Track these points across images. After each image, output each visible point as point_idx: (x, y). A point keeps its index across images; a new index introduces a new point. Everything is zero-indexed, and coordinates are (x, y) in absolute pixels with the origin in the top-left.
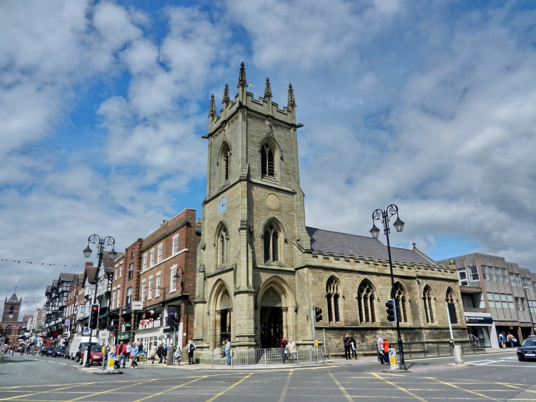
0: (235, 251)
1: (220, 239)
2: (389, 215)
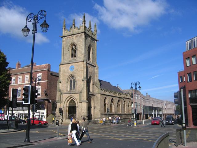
1: (69, 81)
2: (137, 84)
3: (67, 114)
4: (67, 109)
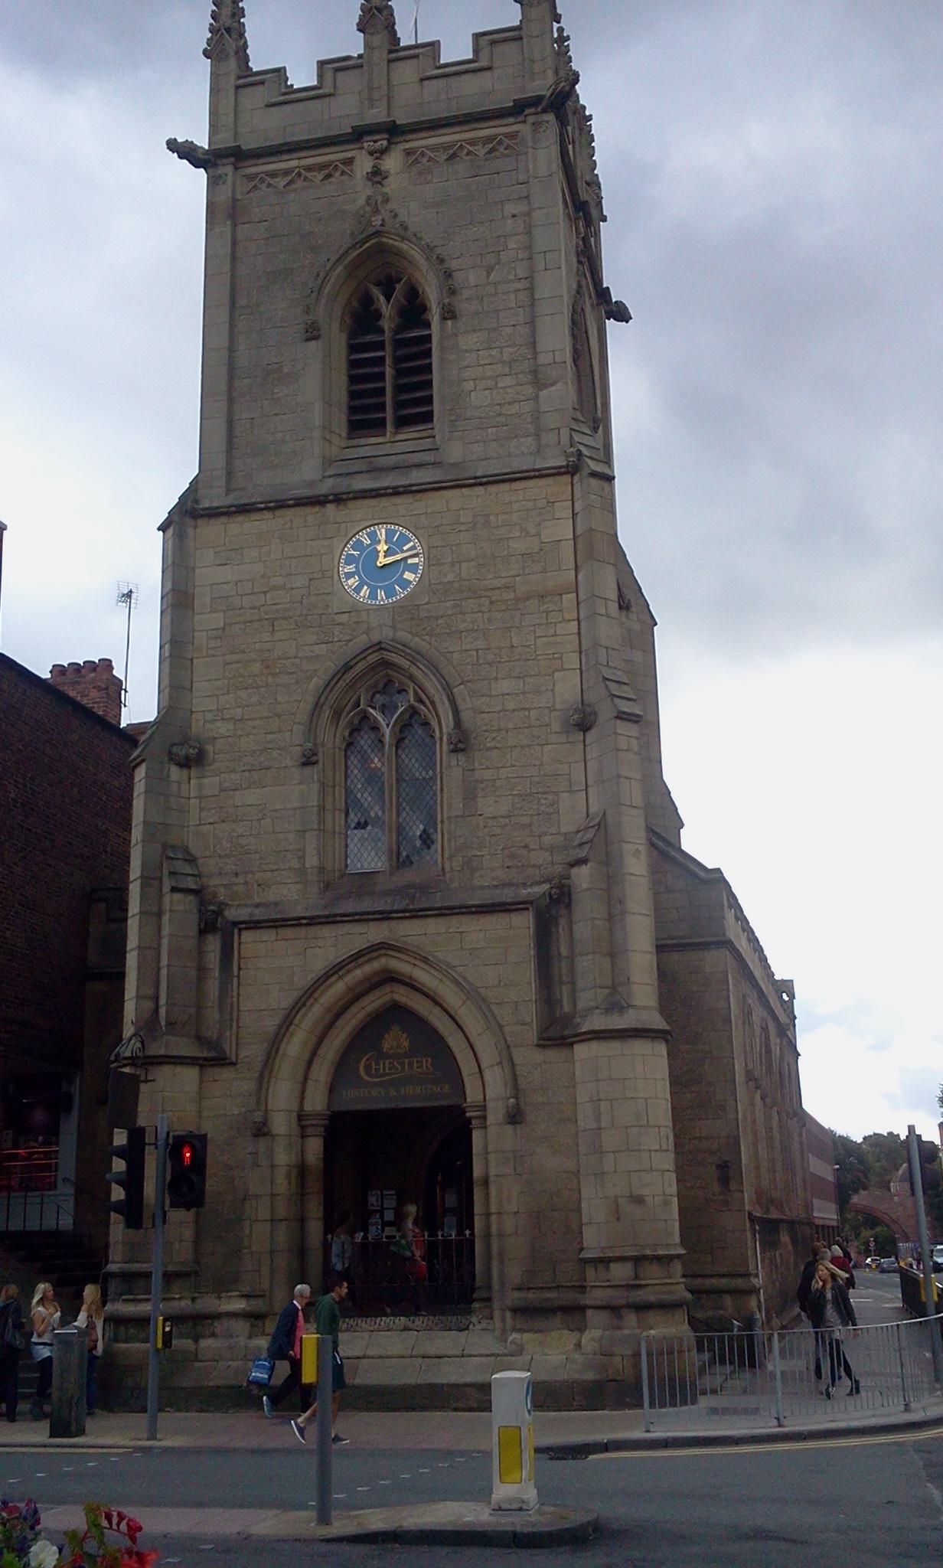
0: (526, 820)
3: (315, 1229)
4: (315, 1147)
